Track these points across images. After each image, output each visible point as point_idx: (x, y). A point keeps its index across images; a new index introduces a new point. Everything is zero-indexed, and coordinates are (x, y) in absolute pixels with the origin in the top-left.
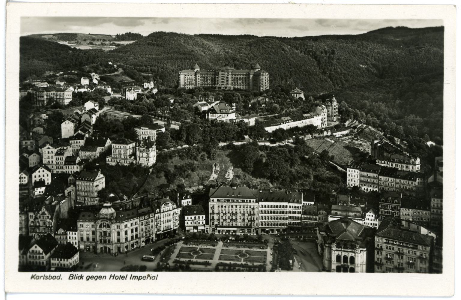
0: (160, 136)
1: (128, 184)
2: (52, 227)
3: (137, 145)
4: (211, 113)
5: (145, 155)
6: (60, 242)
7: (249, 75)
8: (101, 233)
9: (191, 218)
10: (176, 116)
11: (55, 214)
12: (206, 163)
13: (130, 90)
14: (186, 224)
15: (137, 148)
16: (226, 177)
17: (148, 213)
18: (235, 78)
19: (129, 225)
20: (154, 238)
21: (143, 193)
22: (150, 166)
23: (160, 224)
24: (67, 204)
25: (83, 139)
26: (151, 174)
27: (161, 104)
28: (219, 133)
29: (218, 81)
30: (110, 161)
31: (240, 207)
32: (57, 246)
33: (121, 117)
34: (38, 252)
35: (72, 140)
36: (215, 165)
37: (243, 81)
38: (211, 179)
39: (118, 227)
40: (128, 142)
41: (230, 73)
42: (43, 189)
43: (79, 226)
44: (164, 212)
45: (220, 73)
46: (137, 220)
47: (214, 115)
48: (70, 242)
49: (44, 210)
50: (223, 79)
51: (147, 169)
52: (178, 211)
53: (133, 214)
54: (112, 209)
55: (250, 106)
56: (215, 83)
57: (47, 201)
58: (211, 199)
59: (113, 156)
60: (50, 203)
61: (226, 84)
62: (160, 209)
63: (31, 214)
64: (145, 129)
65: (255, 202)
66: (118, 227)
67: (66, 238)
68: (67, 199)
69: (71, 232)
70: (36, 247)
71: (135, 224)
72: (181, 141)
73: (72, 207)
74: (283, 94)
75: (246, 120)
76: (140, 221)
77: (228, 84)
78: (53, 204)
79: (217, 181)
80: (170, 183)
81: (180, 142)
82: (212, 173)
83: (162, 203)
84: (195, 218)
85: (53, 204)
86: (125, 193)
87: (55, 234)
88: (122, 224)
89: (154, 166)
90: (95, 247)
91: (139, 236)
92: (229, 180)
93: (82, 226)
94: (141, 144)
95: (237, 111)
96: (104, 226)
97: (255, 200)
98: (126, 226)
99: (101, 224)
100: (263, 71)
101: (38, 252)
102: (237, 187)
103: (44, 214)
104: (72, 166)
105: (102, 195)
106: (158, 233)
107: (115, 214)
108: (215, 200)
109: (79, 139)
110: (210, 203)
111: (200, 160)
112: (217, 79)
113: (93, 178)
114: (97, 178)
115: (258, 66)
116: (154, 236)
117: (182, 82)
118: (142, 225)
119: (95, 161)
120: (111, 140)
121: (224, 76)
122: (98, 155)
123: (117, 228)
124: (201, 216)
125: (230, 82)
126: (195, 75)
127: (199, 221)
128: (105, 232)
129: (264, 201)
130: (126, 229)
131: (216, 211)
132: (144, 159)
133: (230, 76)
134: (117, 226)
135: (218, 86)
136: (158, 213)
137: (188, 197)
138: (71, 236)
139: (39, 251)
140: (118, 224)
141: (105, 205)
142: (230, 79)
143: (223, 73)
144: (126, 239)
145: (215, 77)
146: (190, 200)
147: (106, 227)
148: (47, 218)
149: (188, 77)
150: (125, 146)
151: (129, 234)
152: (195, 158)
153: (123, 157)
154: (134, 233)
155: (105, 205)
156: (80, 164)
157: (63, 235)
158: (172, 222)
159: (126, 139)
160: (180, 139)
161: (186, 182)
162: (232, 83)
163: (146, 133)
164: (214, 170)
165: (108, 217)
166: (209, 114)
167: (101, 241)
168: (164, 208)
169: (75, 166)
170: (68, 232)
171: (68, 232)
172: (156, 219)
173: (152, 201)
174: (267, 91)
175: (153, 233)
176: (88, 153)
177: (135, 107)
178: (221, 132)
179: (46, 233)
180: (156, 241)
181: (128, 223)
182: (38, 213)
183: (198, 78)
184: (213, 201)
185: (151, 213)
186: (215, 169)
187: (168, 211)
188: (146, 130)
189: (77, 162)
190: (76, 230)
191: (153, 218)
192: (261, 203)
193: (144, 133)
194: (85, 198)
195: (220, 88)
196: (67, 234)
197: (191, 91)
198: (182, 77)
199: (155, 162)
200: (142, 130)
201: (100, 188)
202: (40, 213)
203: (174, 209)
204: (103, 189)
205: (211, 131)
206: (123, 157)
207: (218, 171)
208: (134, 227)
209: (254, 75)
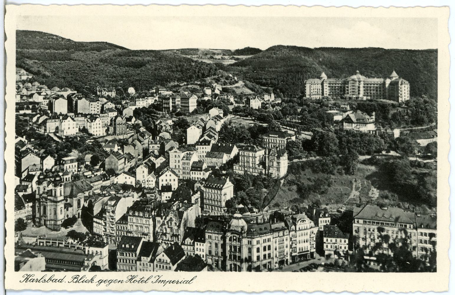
0: (290, 145)
1: (259, 195)
2: (179, 235)
3: (267, 153)
4: (346, 122)
5: (275, 164)
6: (187, 253)
7: (384, 84)
8: (231, 247)
9: (331, 241)
10: (304, 125)
11: (183, 221)
12: (344, 178)
13: (254, 98)
14: (325, 247)
15: (267, 156)
16: (370, 195)
17: (283, 229)
19: (261, 241)
20: (289, 260)
21: (274, 206)
22: (281, 177)
23: (296, 244)
24: (194, 211)
25: (209, 145)
26: (282, 185)
27: (288, 112)
28: (358, 144)
29: (348, 90)
30: (238, 170)
31: (393, 233)
32: (184, 258)
33: (247, 125)
34: (165, 261)
35: (198, 145)
36: (356, 181)
37: (377, 91)
38: (352, 196)
39: (250, 243)
40: (257, 149)
41: (362, 83)
42: (170, 194)
43: (207, 237)
44: (300, 230)
46: (269, 236)
47: (351, 124)
48: (197, 254)
49: (171, 215)
51: (277, 181)
52: (315, 230)
53: (265, 228)
54: (243, 220)
55: (390, 116)
56: (344, 93)
57: (174, 206)
58: (356, 220)
59: (240, 164)
60: (178, 209)
61: (357, 94)
62: (295, 225)
63: (158, 219)
64: (274, 137)
65: (412, 228)
66: (250, 243)
67: (194, 249)
68: (194, 206)
69: (199, 243)
70: (163, 256)
71: (268, 241)
72: (314, 151)
73: (199, 216)
74: (429, 106)
75: (389, 131)
76: (273, 238)
77: (359, 93)
78: (180, 210)
79: (360, 199)
80: (304, 198)
81: (313, 152)
82: (352, 189)
83: (297, 220)
84: (336, 241)
85: (180, 210)
86: (254, 204)
87: (182, 244)
88: (254, 240)
89: (285, 177)
90: (224, 262)
91: (272, 256)
92: (373, 199)
93: (210, 237)
94: (271, 152)
95: (376, 122)
96: (234, 240)
97: (412, 226)
98: (258, 242)
99: (231, 237)
100: (402, 79)
101: (165, 261)
102: (388, 208)
103: (171, 220)
104: (199, 172)
105: (229, 204)
106: (294, 254)
107: (246, 228)
108: (361, 221)
109: (205, 145)
110: (354, 225)
111: (337, 174)
112: (346, 88)
113: (221, 186)
114: (226, 186)
116: (289, 257)
117: (307, 92)
118: (276, 242)
119: (223, 168)
120: (238, 147)
122: (224, 162)
123: (249, 243)
124: (343, 240)
125: (362, 92)
126: (322, 84)
127: (340, 246)
128: (235, 247)
129: (424, 228)
130: (258, 246)
131: (362, 235)
132: (274, 168)
133: (362, 85)
134: (249, 241)
135: (348, 96)
136: (293, 230)
137: (327, 215)
138: (199, 247)
139: (167, 260)
140: (250, 240)
141: (235, 215)
142: (362, 89)
144: (258, 258)
145: (344, 87)
146: (329, 219)
147: (236, 241)
148: (174, 224)
149: (315, 86)
150: (254, 154)
151: (262, 253)
152: (332, 173)
153: (251, 165)
154: (267, 252)
155: (235, 215)
156: (206, 170)
157: (190, 245)
158: (309, 243)
159: (255, 146)
160: (313, 149)
161: (322, 198)
162: (365, 93)
163: (275, 142)
164: (354, 187)
165: (240, 230)
166: (344, 123)
167: (230, 256)
168: (299, 225)
169: (202, 173)
170: (196, 243)
171: (196, 243)
172: (291, 239)
173: (286, 216)
174: (407, 103)
175: (287, 254)
176: (214, 160)
177: (261, 115)
178: (360, 144)
179: (173, 241)
180: (291, 264)
181: (261, 240)
182: (165, 219)
183: (325, 87)
184: (358, 222)
185: (285, 229)
186: (356, 186)
187: (305, 229)
188: (275, 138)
189: (203, 168)
190: (204, 242)
191: (288, 237)
192: (420, 230)
193: (273, 142)
194: (212, 207)
195: (350, 98)
196: (193, 245)
197: (318, 102)
198: (308, 86)
199: (286, 172)
200: (270, 138)
201: (228, 197)
202: (168, 218)
203: (312, 227)
204: (231, 198)
205: (348, 142)
206: (251, 165)
207: (359, 188)
208: (267, 244)
209: (391, 84)
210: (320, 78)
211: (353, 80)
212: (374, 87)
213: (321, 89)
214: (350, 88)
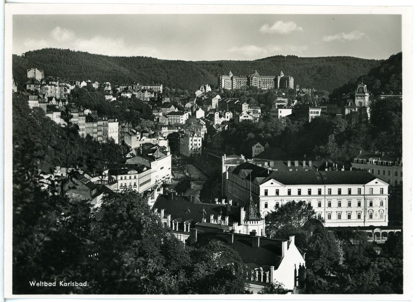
45: (254, 78)
112: (251, 83)
115: (282, 73)
121: (257, 80)
126: (232, 79)
143: (256, 78)
183: (234, 82)
198: (223, 80)
213: (231, 83)
214: (253, 82)
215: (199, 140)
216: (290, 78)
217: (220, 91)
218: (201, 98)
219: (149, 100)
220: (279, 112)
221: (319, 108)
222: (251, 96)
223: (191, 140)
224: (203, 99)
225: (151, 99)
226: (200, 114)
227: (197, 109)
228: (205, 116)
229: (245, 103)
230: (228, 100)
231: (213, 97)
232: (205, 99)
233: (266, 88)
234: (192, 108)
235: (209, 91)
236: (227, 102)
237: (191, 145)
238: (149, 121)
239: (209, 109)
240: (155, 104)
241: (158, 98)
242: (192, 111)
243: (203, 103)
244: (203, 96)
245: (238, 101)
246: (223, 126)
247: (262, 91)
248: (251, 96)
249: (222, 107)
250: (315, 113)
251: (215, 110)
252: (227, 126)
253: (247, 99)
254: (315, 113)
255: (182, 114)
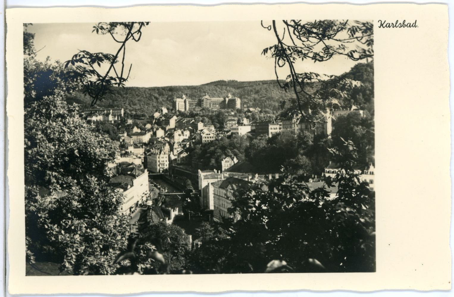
18: (214, 103)
50: (206, 104)
112: (202, 104)
126: (185, 102)
209: (228, 101)
210: (182, 98)
211: (206, 99)
212: (218, 103)
213: (184, 105)
214: (204, 104)
215: (166, 157)
216: (236, 99)
217: (175, 112)
218: (159, 120)
219: (113, 122)
220: (239, 129)
221: (278, 124)
222: (204, 116)
223: (159, 158)
224: (161, 120)
225: (115, 121)
226: (160, 133)
227: (157, 129)
228: (165, 134)
229: (200, 122)
230: (184, 120)
231: (171, 118)
232: (163, 120)
233: (216, 108)
234: (152, 128)
235: (166, 113)
236: (184, 122)
237: (159, 161)
238: (115, 141)
239: (167, 129)
240: (119, 126)
241: (121, 120)
242: (153, 131)
243: (162, 123)
244: (161, 117)
245: (193, 121)
246: (185, 143)
247: (213, 112)
248: (204, 116)
249: (180, 126)
250: (275, 129)
251: (175, 129)
252: (188, 143)
253: (201, 119)
254: (275, 129)
255: (145, 134)
